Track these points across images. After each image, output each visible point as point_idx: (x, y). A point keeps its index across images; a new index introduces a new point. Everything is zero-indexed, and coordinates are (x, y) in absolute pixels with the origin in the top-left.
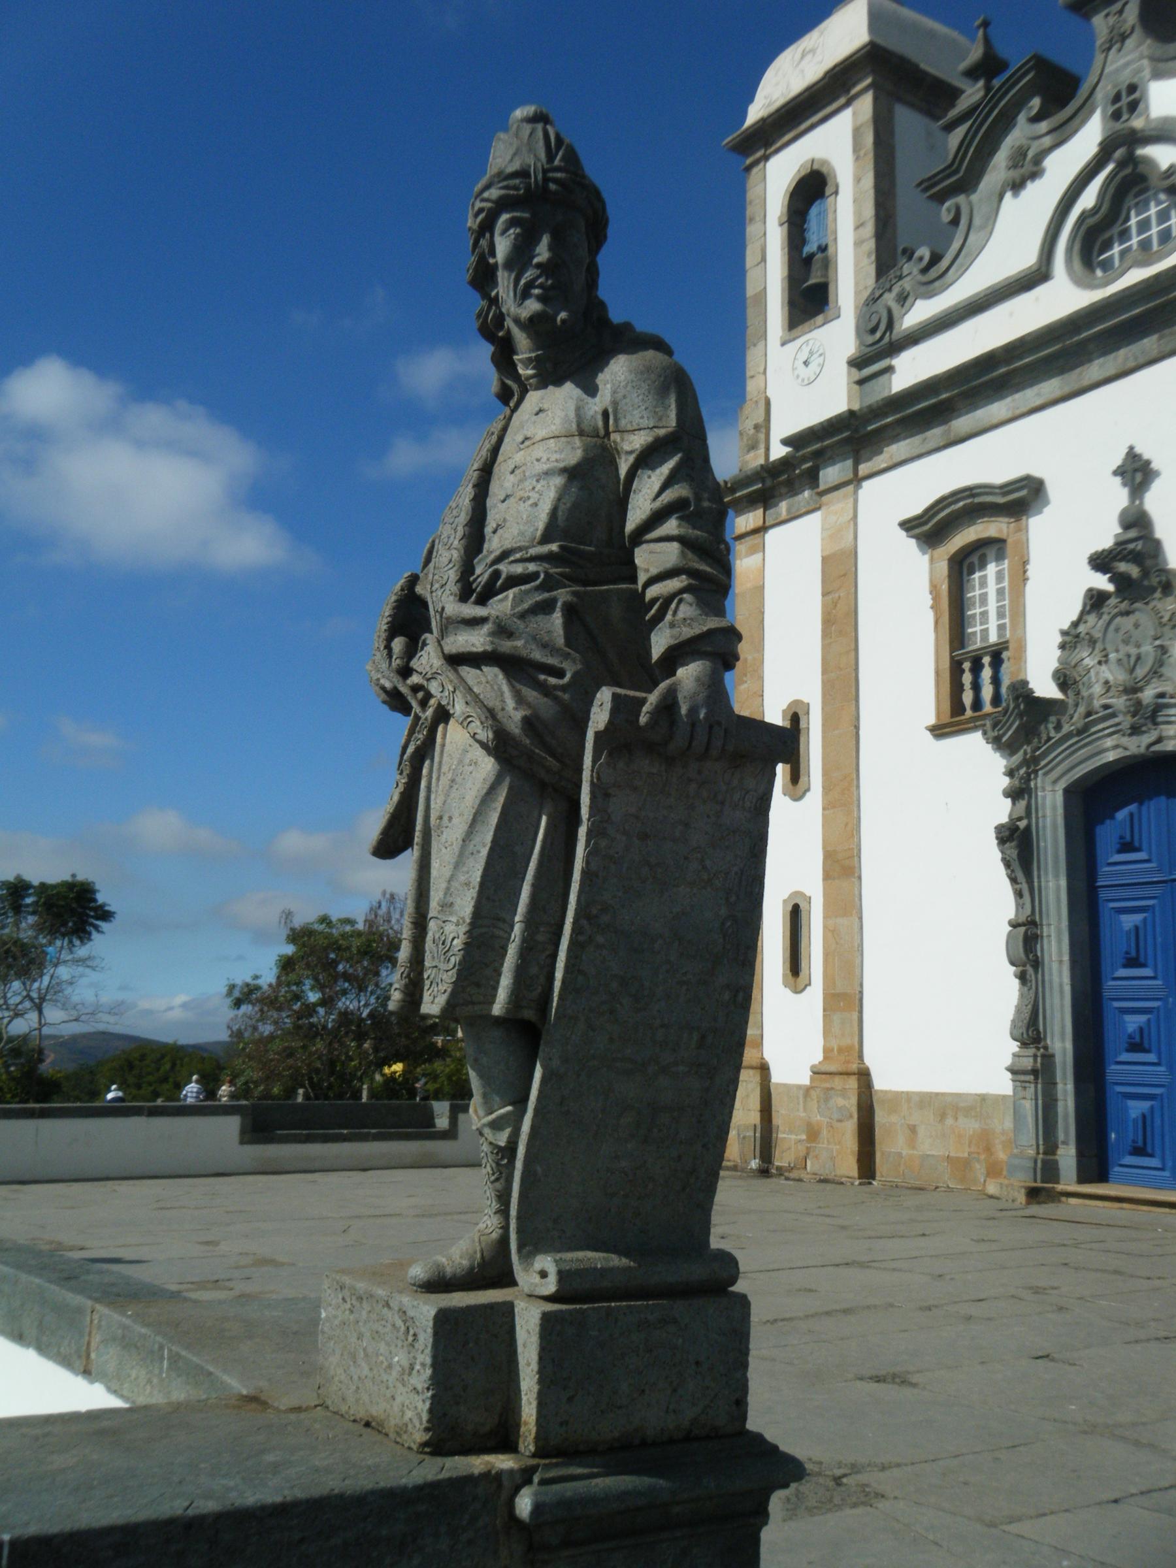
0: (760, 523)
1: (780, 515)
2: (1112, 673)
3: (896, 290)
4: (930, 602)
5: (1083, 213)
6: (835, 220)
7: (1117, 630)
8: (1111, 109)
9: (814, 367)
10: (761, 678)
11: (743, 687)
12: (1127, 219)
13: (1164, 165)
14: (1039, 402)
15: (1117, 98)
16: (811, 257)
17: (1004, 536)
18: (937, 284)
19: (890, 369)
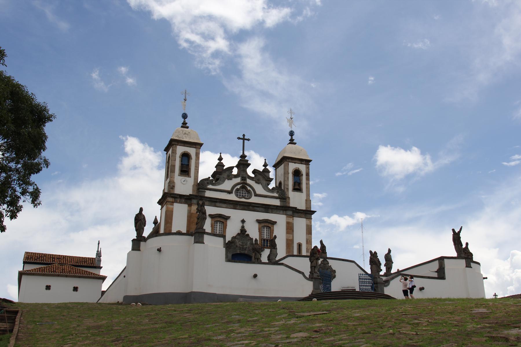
0: (173, 201)
1: (177, 202)
2: (240, 243)
3: (207, 181)
4: (210, 225)
5: (238, 188)
6: (191, 163)
7: (242, 238)
8: (242, 179)
9: (184, 183)
10: (172, 225)
11: (167, 225)
12: (241, 191)
13: (249, 189)
14: (230, 208)
15: (243, 178)
16: (183, 164)
17: (224, 221)
18: (214, 185)
19: (206, 192)
